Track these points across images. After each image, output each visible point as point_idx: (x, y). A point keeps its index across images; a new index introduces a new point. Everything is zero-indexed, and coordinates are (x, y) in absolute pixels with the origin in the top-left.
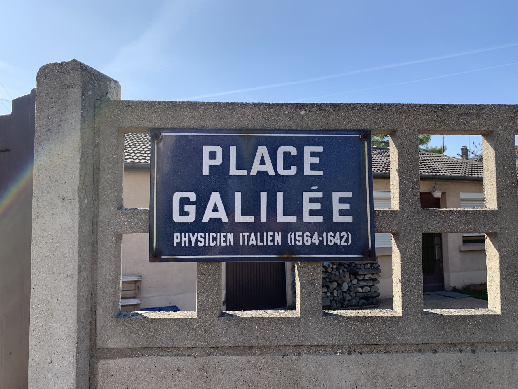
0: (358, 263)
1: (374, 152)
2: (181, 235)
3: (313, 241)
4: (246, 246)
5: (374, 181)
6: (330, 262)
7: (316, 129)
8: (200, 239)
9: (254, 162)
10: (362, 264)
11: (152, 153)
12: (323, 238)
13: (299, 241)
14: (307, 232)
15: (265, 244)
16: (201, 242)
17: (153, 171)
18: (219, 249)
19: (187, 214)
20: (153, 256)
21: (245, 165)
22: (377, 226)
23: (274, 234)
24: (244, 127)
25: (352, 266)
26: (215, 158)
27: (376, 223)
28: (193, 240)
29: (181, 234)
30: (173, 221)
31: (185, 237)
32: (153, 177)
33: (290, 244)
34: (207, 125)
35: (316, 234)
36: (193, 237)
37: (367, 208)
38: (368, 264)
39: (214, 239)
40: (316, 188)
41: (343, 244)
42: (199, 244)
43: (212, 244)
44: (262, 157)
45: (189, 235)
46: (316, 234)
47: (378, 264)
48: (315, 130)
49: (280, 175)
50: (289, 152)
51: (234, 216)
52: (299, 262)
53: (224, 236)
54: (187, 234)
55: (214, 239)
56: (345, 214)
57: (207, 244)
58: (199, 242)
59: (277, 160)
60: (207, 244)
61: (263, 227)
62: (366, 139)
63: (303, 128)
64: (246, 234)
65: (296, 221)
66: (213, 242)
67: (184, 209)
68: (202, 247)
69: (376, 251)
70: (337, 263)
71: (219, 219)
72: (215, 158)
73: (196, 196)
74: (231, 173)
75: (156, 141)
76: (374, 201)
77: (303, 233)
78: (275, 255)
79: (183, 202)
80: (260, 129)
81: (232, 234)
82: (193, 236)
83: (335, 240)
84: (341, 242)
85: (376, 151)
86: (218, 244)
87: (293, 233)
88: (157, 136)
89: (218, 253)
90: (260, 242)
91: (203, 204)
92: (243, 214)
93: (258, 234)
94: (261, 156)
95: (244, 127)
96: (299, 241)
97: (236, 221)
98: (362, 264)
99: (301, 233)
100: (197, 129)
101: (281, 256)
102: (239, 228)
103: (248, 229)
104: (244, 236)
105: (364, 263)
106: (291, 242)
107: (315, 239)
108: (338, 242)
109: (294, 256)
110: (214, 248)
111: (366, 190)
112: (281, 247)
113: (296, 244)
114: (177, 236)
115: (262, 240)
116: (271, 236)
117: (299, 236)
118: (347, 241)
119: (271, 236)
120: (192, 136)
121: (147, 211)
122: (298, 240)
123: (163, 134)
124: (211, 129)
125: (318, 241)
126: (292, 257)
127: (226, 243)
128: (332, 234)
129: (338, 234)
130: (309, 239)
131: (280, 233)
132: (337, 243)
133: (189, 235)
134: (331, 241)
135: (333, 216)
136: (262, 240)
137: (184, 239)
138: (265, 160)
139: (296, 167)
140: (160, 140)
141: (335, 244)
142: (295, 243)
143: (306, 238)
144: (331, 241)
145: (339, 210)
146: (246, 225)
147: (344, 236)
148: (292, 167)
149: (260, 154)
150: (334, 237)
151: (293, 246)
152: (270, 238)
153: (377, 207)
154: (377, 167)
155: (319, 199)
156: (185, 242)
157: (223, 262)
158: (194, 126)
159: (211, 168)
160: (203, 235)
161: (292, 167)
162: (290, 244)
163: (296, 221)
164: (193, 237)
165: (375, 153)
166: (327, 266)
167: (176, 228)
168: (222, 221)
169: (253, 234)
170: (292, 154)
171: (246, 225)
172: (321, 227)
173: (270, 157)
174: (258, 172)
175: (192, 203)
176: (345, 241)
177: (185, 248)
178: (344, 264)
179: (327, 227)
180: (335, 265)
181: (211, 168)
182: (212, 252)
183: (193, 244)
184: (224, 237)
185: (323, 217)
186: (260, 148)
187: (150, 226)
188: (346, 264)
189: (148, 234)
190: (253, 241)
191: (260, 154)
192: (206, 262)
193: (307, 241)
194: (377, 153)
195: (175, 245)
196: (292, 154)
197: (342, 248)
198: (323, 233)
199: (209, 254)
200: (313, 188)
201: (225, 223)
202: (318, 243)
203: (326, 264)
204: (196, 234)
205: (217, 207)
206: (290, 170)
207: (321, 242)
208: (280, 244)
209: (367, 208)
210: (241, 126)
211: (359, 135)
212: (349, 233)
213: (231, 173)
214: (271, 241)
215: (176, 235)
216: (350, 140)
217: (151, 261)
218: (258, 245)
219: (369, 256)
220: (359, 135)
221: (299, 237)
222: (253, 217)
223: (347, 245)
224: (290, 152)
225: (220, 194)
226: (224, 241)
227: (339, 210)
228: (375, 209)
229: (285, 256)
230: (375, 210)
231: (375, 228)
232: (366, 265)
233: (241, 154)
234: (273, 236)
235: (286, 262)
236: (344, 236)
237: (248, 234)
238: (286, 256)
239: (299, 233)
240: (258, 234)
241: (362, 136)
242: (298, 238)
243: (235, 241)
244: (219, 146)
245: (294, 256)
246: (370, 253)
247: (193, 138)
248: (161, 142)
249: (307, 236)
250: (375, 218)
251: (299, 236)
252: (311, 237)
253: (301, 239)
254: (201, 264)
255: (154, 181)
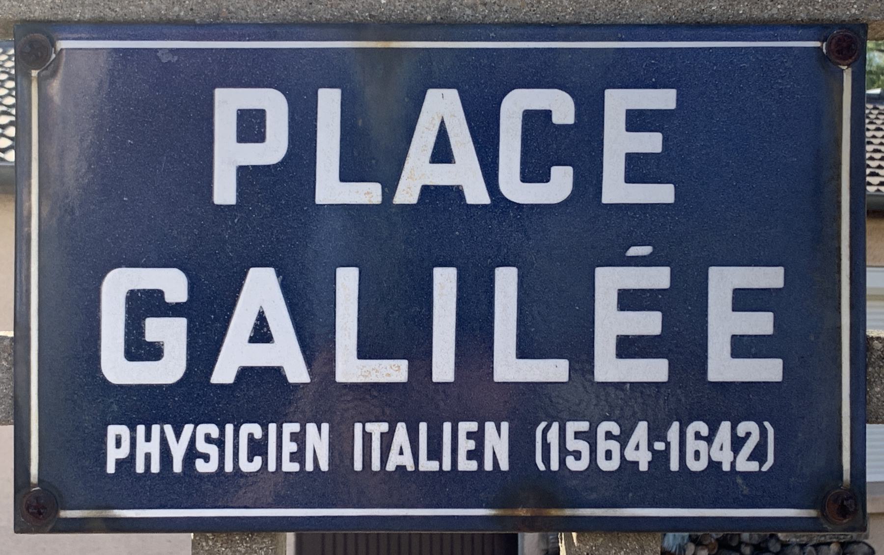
0: (794, 540)
1: (871, 113)
2: (131, 432)
3: (630, 455)
4: (376, 472)
5: (871, 226)
6: (686, 534)
7: (651, 21)
8: (201, 446)
9: (410, 152)
10: (805, 545)
11: (21, 122)
12: (668, 445)
13: (577, 455)
14: (608, 419)
15: (447, 466)
16: (206, 458)
17: (25, 191)
18: (275, 485)
19: (154, 352)
20: (28, 509)
21: (373, 162)
22: (875, 400)
23: (482, 428)
24: (370, 16)
25: (770, 552)
26: (261, 138)
27: (872, 388)
28: (178, 451)
29: (133, 430)
30: (105, 380)
31: (148, 439)
32: (25, 213)
33: (542, 467)
34: (231, 8)
35: (642, 429)
36: (178, 441)
37: (839, 328)
38: (829, 544)
39: (257, 448)
40: (645, 250)
41: (745, 465)
42: (201, 466)
43: (246, 467)
44: (439, 131)
45: (162, 432)
46: (642, 429)
47: (870, 547)
48: (649, 25)
49: (510, 201)
50: (546, 111)
51: (332, 360)
52: (574, 535)
53: (294, 437)
54: (156, 429)
55: (257, 448)
56: (753, 350)
57: (229, 467)
58: (199, 457)
59: (498, 144)
60: (229, 467)
61: (442, 404)
62: (845, 59)
63: (600, 17)
64: (377, 429)
65: (565, 378)
66: (250, 460)
67: (142, 334)
68: (209, 476)
69: (868, 497)
70: (713, 541)
71: (277, 373)
72: (261, 138)
73: (189, 284)
74: (321, 198)
75: (34, 73)
76: (868, 303)
77: (590, 425)
78: (486, 508)
79: (141, 309)
80: (434, 24)
81: (325, 427)
82: (178, 435)
83: (712, 450)
84: (735, 458)
85: (875, 108)
86: (272, 467)
87: (555, 426)
88: (39, 54)
89: (270, 500)
90: (430, 458)
91: (214, 313)
92: (365, 352)
93: (423, 427)
94: (440, 122)
95: (373, 13)
96: (577, 455)
97: (340, 378)
98: (805, 545)
99: (584, 426)
100: (191, 24)
101: (509, 512)
102: (350, 405)
103: (383, 412)
104: (367, 437)
105: (814, 542)
106: (546, 459)
107: (637, 448)
108: (725, 458)
109: (555, 512)
110: (254, 483)
111: (840, 259)
112: (509, 478)
113: (565, 464)
114: (117, 435)
115: (435, 453)
116: (470, 435)
117: (578, 435)
118: (758, 455)
119: (470, 435)
120: (172, 51)
121: (6, 343)
122: (574, 451)
123: (63, 44)
124: (244, 21)
125: (648, 456)
126: (546, 517)
127: (302, 463)
128: (703, 428)
129: (726, 426)
130: (615, 446)
131: (505, 426)
132: (720, 463)
133: (162, 432)
134: (697, 455)
135: (710, 361)
136: (435, 453)
137: (142, 447)
138: (452, 141)
139: (570, 170)
140: (50, 68)
141: (715, 466)
142: (562, 462)
143: (603, 445)
144: (697, 455)
145: (733, 337)
146: (375, 393)
147: (748, 434)
148: (556, 171)
149: (433, 118)
150: (709, 440)
151: (555, 472)
152: (290, 447)
153: (875, 327)
154: (877, 171)
155: (657, 296)
156: (148, 457)
157: (288, 534)
158: (182, 13)
159: (245, 174)
160: (213, 430)
161: (556, 171)
162: (542, 467)
163: (565, 378)
164: (178, 441)
165: (871, 116)
166: (673, 550)
167: (115, 407)
168: (285, 378)
169: (401, 429)
170: (557, 119)
171: (375, 393)
172: (661, 402)
173: (471, 134)
174: (425, 189)
175: (175, 310)
176: (751, 455)
177: (149, 483)
178: (741, 543)
179: (683, 400)
180: (707, 546)
181: (245, 174)
182: (249, 495)
183: (178, 467)
184: (291, 440)
185: (670, 364)
186: (433, 97)
187: (15, 398)
188: (747, 544)
189: (11, 428)
190: (401, 453)
191: (433, 118)
192: (226, 532)
193: (609, 455)
194: (873, 112)
195: (111, 468)
196: (557, 119)
197: (739, 481)
198: (668, 426)
199: (235, 505)
200: (634, 251)
201: (297, 386)
202: (649, 463)
203: (671, 544)
204: (188, 429)
205: (267, 326)
206: (548, 181)
207: (660, 459)
208: (504, 466)
209: (840, 328)
210: (360, 13)
211: (817, 44)
212: (767, 424)
213: (321, 198)
214: (471, 455)
215: (113, 430)
216: (782, 62)
217: (20, 528)
218: (421, 469)
219: (844, 512)
220: (817, 44)
221: (576, 438)
222: (404, 364)
223: (757, 469)
224: (548, 114)
225: (278, 277)
226: (292, 454)
227: (733, 337)
228: (871, 332)
229: (522, 512)
230: (872, 338)
231: (869, 407)
232: (825, 548)
233: (360, 123)
234: (478, 437)
235: (520, 535)
236: (748, 434)
237: (384, 427)
238: (525, 510)
239: (576, 423)
240: (423, 427)
241: (833, 47)
242: (572, 444)
243: (336, 454)
244: (276, 88)
245: (555, 512)
246: (847, 500)
247: (176, 58)
248: (54, 74)
249: (609, 436)
250: (870, 369)
251: (578, 435)
252: (623, 439)
253: (583, 446)
254: (207, 539)
255: (29, 226)
